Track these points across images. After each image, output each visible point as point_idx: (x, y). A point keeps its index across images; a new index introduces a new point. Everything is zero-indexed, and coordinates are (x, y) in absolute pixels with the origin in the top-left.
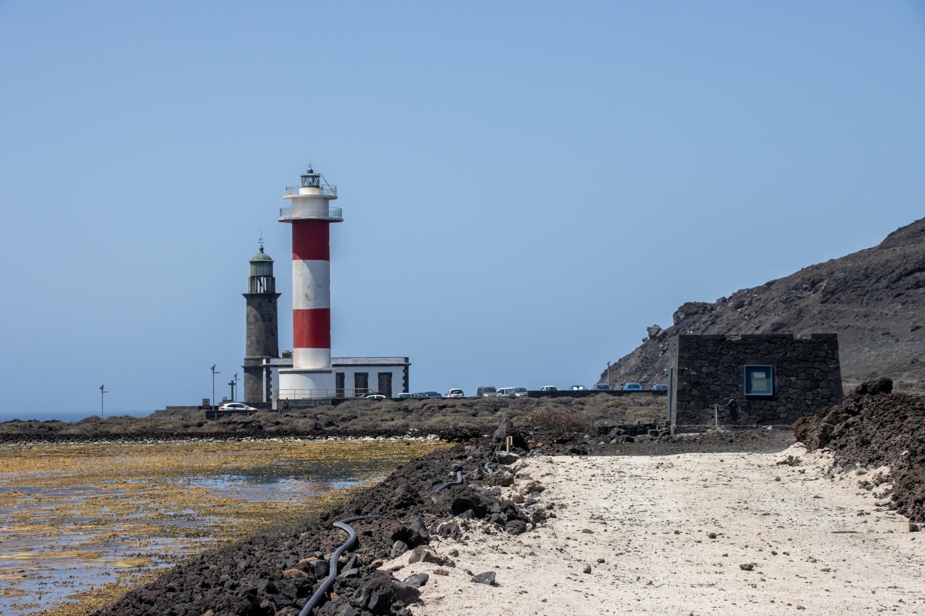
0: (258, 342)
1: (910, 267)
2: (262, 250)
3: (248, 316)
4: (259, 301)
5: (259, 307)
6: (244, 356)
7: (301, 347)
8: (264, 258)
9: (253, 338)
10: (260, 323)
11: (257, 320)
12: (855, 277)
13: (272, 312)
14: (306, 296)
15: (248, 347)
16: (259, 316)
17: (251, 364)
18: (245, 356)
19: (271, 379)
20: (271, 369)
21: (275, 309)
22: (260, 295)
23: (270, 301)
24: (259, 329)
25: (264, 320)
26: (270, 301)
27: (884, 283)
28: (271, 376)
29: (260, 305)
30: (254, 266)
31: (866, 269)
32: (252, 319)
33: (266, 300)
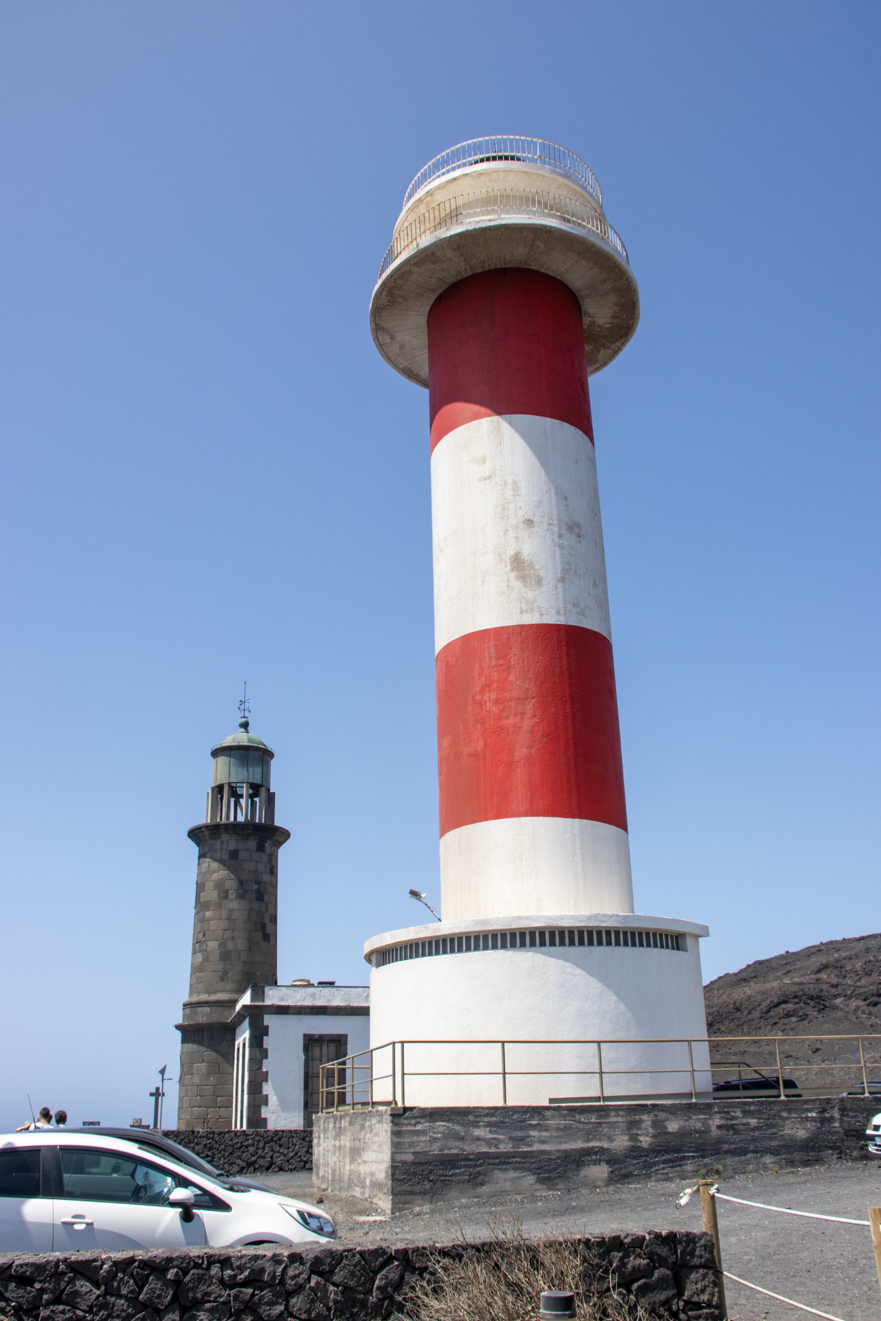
0: (225, 956)
1: (776, 1000)
2: (245, 726)
3: (200, 887)
4: (230, 843)
5: (232, 860)
6: (185, 996)
7: (501, 814)
8: (250, 740)
9: (213, 945)
10: (234, 904)
11: (224, 895)
12: (726, 1010)
13: (266, 877)
14: (518, 563)
15: (196, 970)
16: (231, 884)
17: (203, 1016)
18: (185, 998)
19: (265, 1054)
20: (269, 1020)
21: (273, 870)
22: (235, 828)
23: (260, 848)
24: (229, 919)
25: (241, 897)
26: (260, 848)
27: (756, 1014)
28: (267, 1042)
29: (234, 854)
30: (222, 760)
31: (735, 1003)
32: (211, 894)
33: (252, 844)
